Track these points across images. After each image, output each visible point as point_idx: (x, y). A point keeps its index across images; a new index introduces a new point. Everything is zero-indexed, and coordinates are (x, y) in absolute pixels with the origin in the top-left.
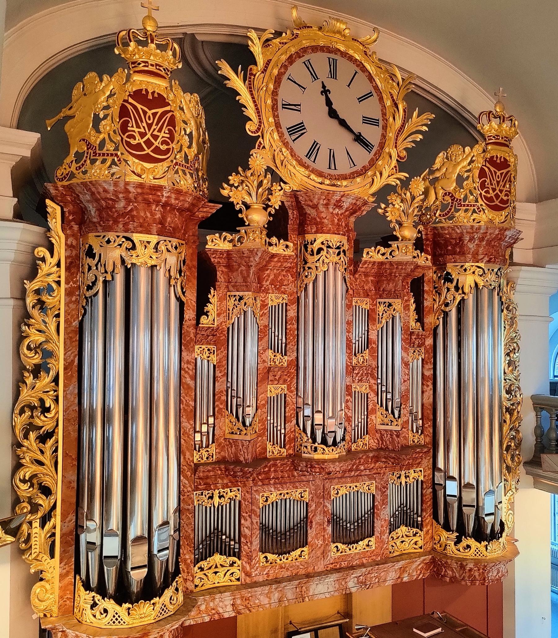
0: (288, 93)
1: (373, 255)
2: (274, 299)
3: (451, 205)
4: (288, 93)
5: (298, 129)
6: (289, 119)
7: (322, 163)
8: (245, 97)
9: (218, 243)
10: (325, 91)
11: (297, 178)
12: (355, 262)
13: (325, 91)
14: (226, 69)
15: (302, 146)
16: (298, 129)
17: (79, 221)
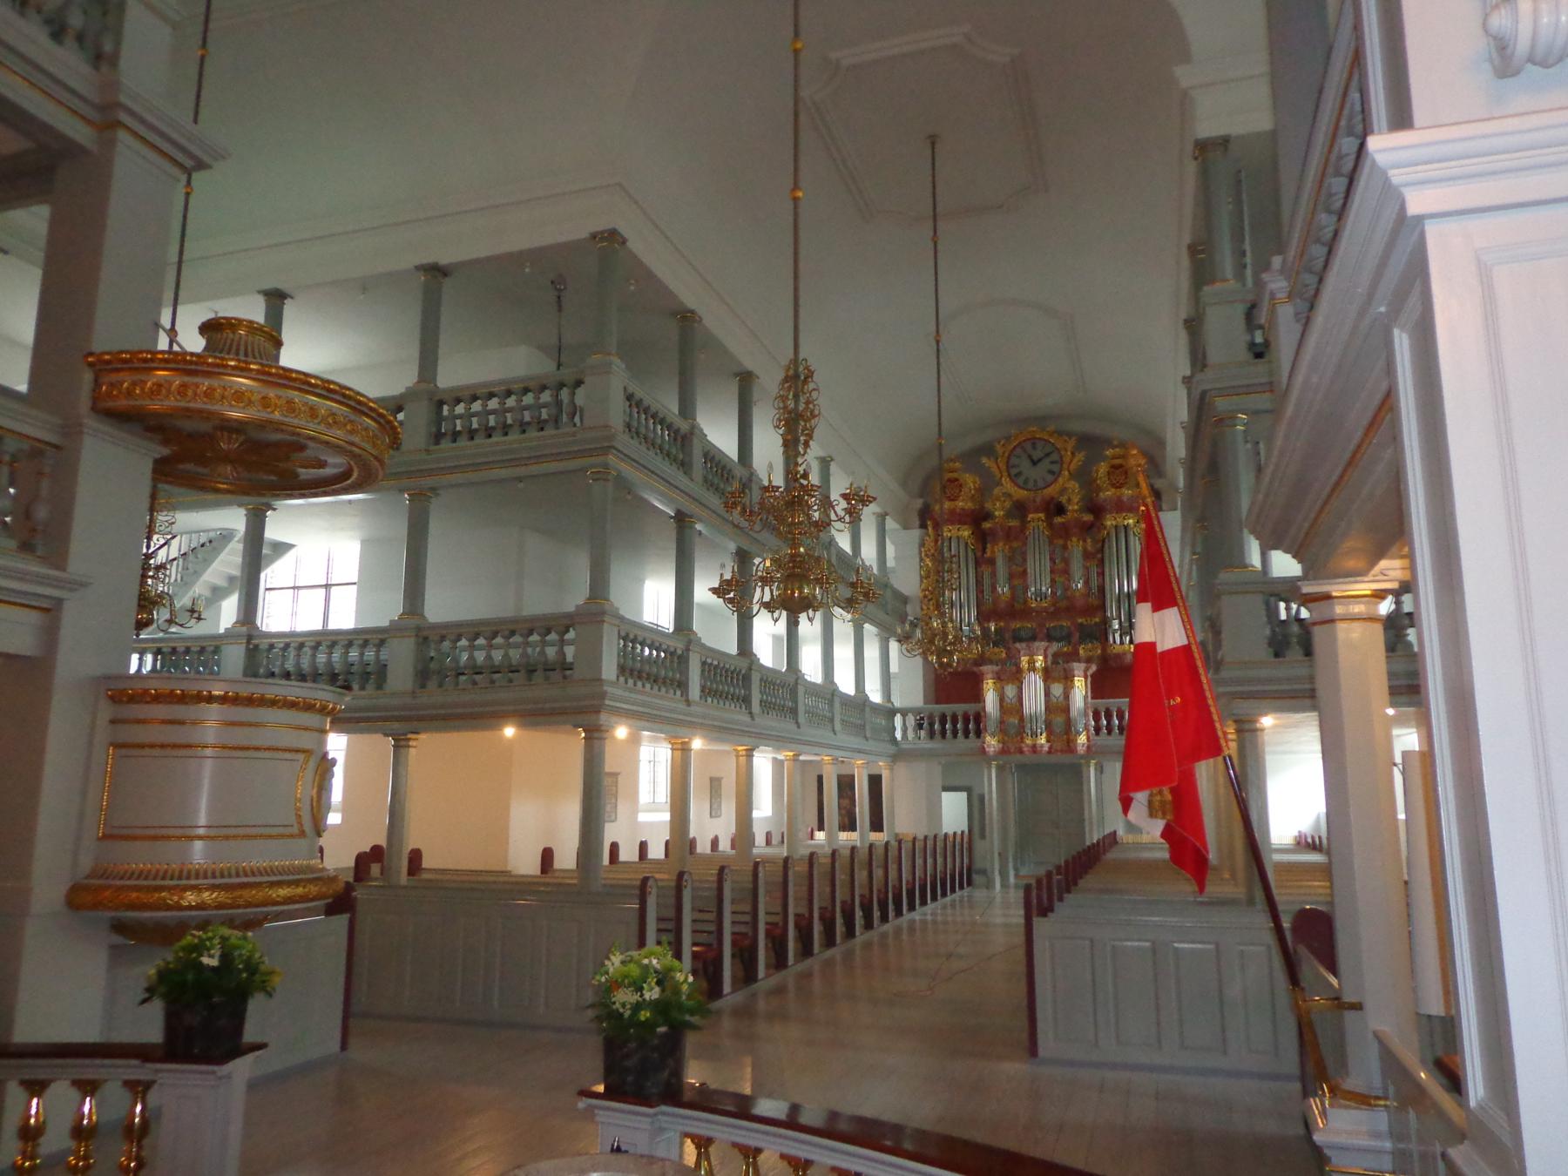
0: (1014, 461)
1: (1058, 520)
2: (1015, 545)
3: (1099, 489)
4: (1014, 461)
5: (1019, 474)
6: (1014, 471)
7: (1031, 485)
8: (994, 469)
9: (987, 525)
10: (1030, 457)
11: (1020, 494)
12: (1051, 525)
13: (1030, 457)
14: (984, 460)
15: (1020, 481)
16: (1019, 474)
17: (937, 526)
